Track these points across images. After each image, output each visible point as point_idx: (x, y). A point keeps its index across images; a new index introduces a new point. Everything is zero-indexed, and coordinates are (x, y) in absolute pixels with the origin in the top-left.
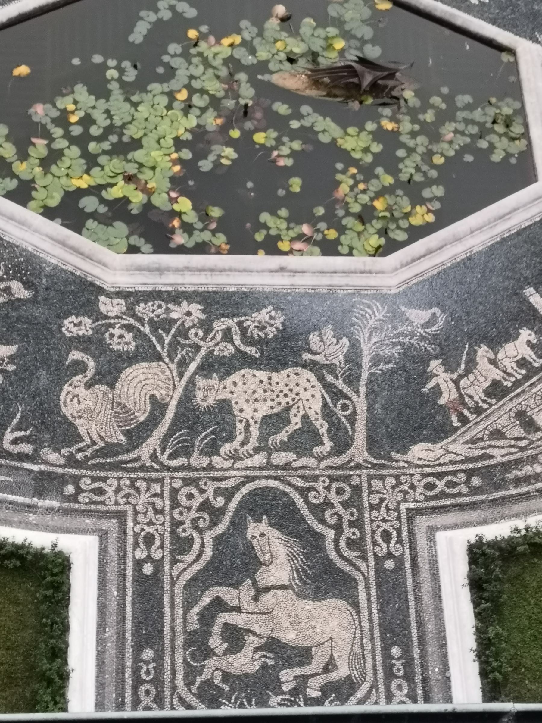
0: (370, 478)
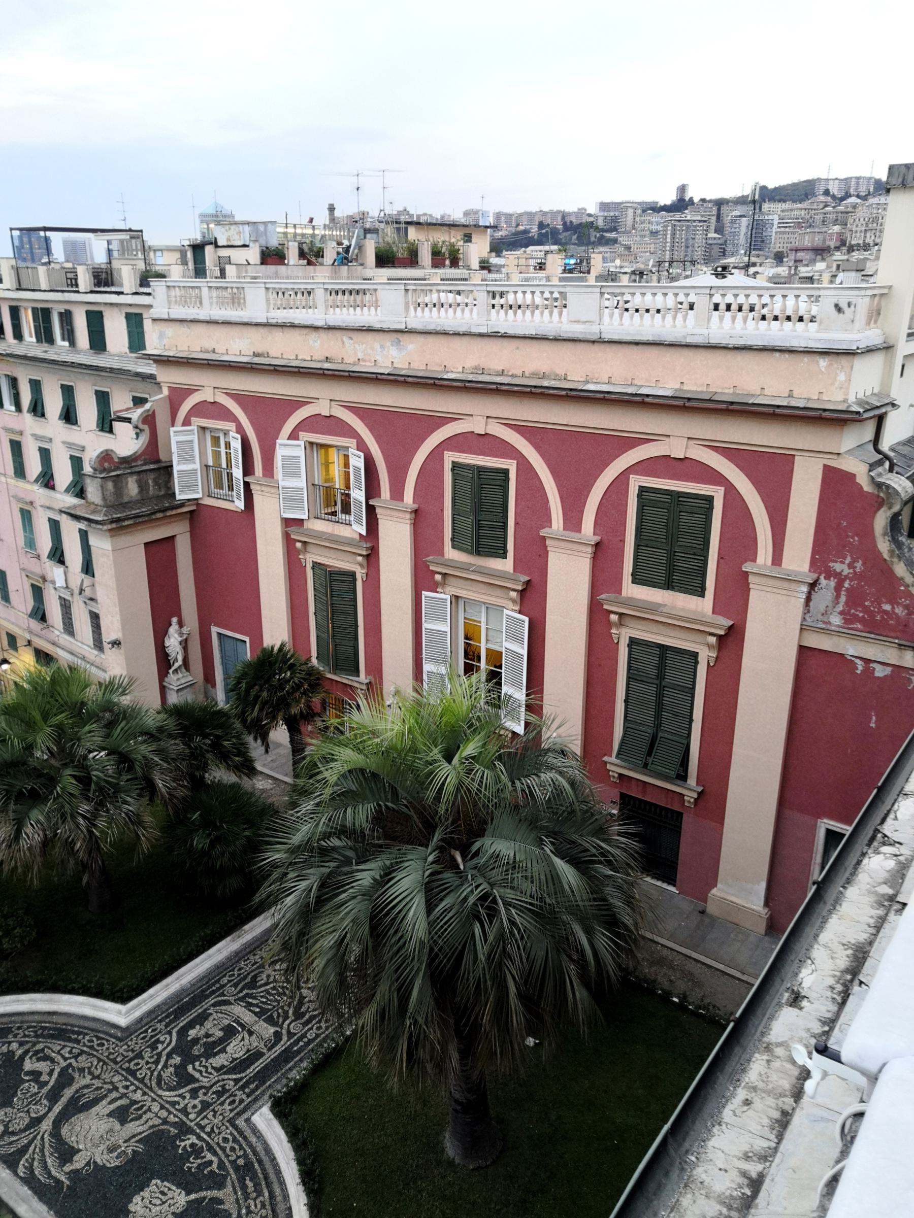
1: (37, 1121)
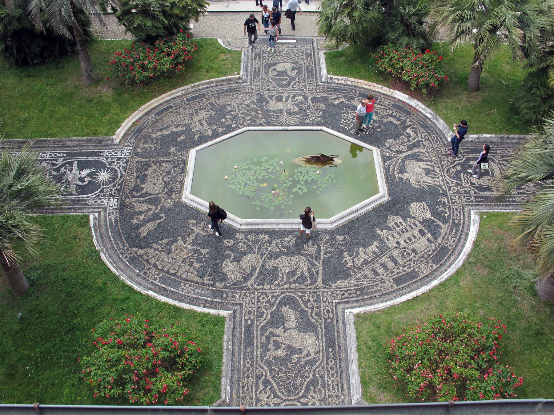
0: (323, 292)
1: (401, 152)
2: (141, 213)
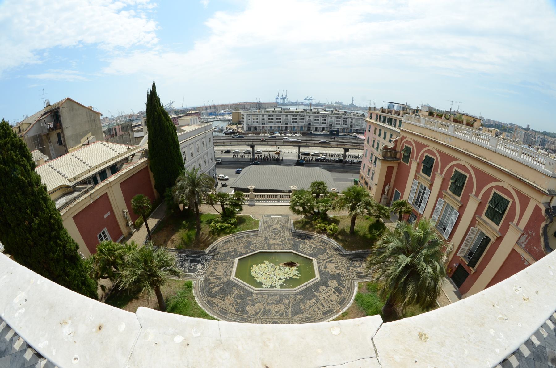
2: (213, 283)
